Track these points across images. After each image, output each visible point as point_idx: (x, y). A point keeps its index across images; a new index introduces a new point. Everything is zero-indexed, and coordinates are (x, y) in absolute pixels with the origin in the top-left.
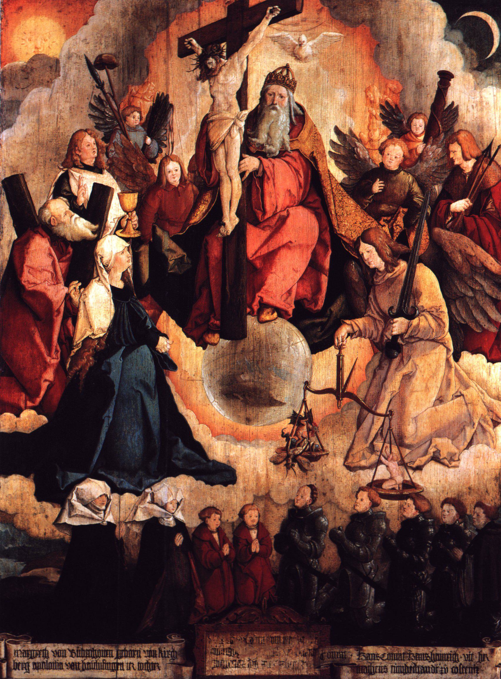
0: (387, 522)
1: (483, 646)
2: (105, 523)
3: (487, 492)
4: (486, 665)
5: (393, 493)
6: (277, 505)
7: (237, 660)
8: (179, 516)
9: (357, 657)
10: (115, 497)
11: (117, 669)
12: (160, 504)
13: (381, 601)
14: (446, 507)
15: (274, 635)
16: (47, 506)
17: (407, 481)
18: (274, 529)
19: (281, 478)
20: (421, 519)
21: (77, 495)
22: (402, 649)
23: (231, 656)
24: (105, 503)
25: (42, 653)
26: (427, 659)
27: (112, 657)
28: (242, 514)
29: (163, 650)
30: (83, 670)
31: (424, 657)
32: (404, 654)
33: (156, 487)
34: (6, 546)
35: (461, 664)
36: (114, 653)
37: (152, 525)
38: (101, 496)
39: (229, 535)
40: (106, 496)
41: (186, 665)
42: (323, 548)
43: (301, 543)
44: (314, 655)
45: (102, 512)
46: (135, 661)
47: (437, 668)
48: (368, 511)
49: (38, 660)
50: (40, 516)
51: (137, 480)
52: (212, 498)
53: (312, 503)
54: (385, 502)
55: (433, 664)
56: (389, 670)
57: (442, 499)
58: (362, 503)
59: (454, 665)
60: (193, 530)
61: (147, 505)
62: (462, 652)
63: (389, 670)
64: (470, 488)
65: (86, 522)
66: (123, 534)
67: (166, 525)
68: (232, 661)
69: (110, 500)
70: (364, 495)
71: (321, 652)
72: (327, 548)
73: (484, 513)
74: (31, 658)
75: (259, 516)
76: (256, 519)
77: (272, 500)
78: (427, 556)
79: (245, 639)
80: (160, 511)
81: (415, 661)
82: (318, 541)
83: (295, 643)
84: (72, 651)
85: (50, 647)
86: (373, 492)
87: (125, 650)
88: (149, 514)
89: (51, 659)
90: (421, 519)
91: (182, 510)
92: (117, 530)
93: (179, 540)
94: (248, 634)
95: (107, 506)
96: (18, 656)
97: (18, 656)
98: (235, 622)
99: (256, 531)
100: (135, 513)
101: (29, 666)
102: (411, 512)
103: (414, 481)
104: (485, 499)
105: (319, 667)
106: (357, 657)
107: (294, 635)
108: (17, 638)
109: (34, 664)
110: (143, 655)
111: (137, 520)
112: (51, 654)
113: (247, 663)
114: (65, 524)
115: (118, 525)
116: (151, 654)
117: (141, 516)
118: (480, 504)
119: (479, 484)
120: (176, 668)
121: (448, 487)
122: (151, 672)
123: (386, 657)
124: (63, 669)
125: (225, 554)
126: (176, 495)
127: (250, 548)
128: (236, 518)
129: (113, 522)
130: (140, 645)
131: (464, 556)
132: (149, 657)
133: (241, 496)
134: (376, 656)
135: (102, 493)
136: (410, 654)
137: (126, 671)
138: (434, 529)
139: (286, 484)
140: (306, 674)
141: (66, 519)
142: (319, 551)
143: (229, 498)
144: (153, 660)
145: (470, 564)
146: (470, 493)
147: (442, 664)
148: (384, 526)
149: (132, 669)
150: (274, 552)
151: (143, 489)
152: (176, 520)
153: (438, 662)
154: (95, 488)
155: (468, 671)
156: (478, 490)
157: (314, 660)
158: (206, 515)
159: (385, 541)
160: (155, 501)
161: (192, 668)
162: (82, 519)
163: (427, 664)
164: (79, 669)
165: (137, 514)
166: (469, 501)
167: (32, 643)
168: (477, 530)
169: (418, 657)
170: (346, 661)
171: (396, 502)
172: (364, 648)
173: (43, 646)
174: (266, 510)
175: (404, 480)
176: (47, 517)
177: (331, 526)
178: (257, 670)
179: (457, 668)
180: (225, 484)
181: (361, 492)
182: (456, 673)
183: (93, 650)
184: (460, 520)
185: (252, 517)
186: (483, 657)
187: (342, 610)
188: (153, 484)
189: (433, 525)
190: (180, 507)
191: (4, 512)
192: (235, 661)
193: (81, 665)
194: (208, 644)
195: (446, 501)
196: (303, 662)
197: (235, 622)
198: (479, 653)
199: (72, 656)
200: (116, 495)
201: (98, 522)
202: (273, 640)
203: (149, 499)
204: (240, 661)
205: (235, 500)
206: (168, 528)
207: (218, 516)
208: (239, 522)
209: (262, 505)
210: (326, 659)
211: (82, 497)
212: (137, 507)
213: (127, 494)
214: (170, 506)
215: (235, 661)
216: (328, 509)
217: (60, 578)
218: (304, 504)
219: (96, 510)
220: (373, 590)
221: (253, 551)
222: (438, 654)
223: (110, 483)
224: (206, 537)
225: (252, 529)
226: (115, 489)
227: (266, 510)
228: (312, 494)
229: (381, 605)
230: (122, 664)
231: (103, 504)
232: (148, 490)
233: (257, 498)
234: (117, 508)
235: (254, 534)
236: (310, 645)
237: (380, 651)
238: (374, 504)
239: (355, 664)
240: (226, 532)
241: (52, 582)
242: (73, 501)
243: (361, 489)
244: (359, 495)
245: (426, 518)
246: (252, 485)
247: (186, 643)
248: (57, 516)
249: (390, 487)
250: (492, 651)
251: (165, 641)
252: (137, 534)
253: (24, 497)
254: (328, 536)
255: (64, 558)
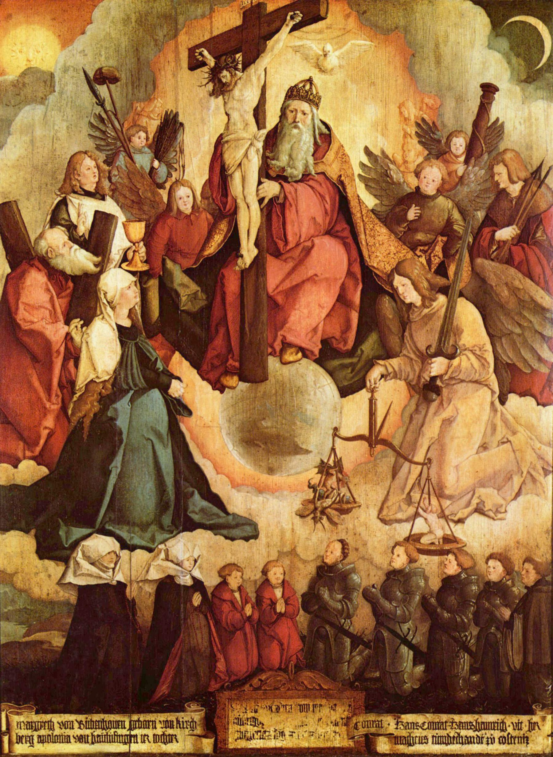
0: (426, 579)
1: (531, 712)
2: (114, 583)
3: (537, 546)
4: (537, 734)
5: (433, 548)
6: (305, 562)
7: (262, 730)
8: (197, 573)
9: (395, 726)
10: (125, 554)
11: (131, 742)
12: (175, 561)
13: (421, 663)
14: (491, 563)
15: (303, 703)
16: (50, 564)
17: (447, 535)
18: (301, 585)
19: (308, 532)
20: (463, 576)
21: (83, 553)
22: (444, 717)
23: (255, 726)
24: (114, 561)
25: (47, 724)
26: (471, 728)
27: (125, 728)
28: (265, 572)
29: (181, 720)
30: (93, 743)
31: (468, 726)
32: (446, 722)
33: (169, 543)
34: (6, 608)
35: (509, 734)
36: (127, 725)
37: (167, 585)
38: (109, 553)
39: (253, 596)
40: (115, 553)
41: (205, 736)
42: (356, 609)
43: (331, 603)
44: (346, 724)
45: (111, 570)
46: (150, 732)
47: (482, 738)
48: (406, 568)
49: (43, 732)
50: (42, 575)
51: (148, 535)
52: (233, 554)
53: (343, 559)
54: (423, 559)
55: (479, 734)
56: (430, 740)
57: (487, 555)
58: (398, 559)
59: (502, 734)
60: (212, 589)
61: (160, 562)
62: (510, 720)
63: (430, 740)
64: (518, 542)
65: (93, 582)
66: (134, 594)
67: (182, 583)
68: (257, 732)
69: (120, 557)
70: (400, 550)
71: (355, 722)
72: (360, 606)
73: (534, 569)
74: (36, 730)
75: (285, 573)
76: (282, 577)
77: (298, 555)
78: (471, 616)
79: (270, 708)
80: (175, 569)
81: (458, 731)
82: (350, 600)
83: (326, 711)
84: (80, 723)
85: (56, 718)
86: (411, 548)
87: (139, 720)
88: (164, 572)
89: (57, 731)
90: (463, 576)
91: (200, 567)
92: (128, 590)
93: (197, 600)
94: (274, 702)
95: (116, 564)
96: (21, 728)
97: (21, 728)
98: (259, 688)
99: (281, 590)
100: (147, 572)
101: (33, 739)
102: (452, 569)
103: (456, 535)
104: (535, 554)
105: (353, 738)
106: (395, 726)
107: (324, 702)
108: (20, 709)
109: (39, 737)
110: (158, 726)
111: (150, 579)
112: (56, 726)
113: (272, 734)
114: (70, 583)
115: (129, 584)
116: (168, 724)
117: (155, 575)
118: (528, 560)
119: (528, 537)
120: (196, 740)
121: (493, 541)
122: (168, 745)
123: (426, 726)
124: (70, 742)
125: (248, 615)
126: (193, 551)
127: (275, 609)
128: (259, 575)
129: (123, 580)
130: (155, 714)
131: (512, 616)
132: (166, 728)
133: (264, 551)
134: (415, 725)
135: (110, 551)
136: (452, 723)
137: (140, 744)
138: (478, 586)
139: (314, 538)
140: (338, 745)
141: (70, 578)
142: (351, 611)
143: (250, 555)
144: (170, 731)
145: (518, 625)
146: (518, 547)
147: (488, 733)
148: (422, 583)
149: (147, 741)
150: (301, 612)
151: (156, 544)
152: (194, 578)
153: (483, 732)
154: (101, 545)
155: (516, 741)
156: (527, 544)
157: (348, 731)
158: (227, 572)
159: (424, 601)
160: (170, 558)
161: (213, 740)
162: (89, 578)
163: (471, 733)
164: (88, 742)
165: (150, 572)
166: (517, 557)
167: (36, 714)
168: (526, 587)
169: (461, 725)
170: (382, 731)
171: (436, 559)
172: (403, 716)
173: (48, 717)
174: (292, 567)
175: (444, 534)
176: (49, 576)
177: (364, 584)
178: (284, 742)
179: (504, 737)
180: (246, 539)
181: (397, 547)
182: (504, 744)
183: (103, 721)
184: (508, 577)
185: (276, 575)
186: (533, 726)
187: (377, 674)
188: (167, 540)
189: (477, 583)
190: (197, 564)
191: (3, 572)
192: (260, 731)
193: (90, 738)
194: (230, 713)
195: (491, 556)
196: (335, 732)
197: (259, 688)
198: (529, 721)
199: (80, 728)
200: (126, 552)
201: (106, 582)
202: (303, 708)
203: (163, 555)
204: (265, 732)
205: (257, 557)
206: (185, 587)
207: (240, 574)
208: (262, 580)
209: (287, 562)
210: (361, 729)
211: (88, 554)
212: (150, 565)
213: (138, 551)
214: (187, 564)
215: (260, 731)
216: (362, 566)
217: (66, 643)
218: (334, 560)
219: (104, 569)
220: (411, 653)
221: (278, 610)
222: (483, 723)
223: (119, 539)
224: (226, 596)
225: (277, 587)
226: (124, 545)
227: (292, 567)
228: (343, 549)
229: (420, 668)
230: (136, 736)
231: (111, 562)
232: (162, 546)
233: (281, 554)
234: (127, 566)
235: (278, 593)
236: (341, 712)
237: (419, 718)
238: (412, 560)
239: (393, 734)
240: (248, 590)
241: (57, 647)
242: (78, 559)
243: (397, 544)
244: (395, 551)
245: (469, 576)
246: (276, 539)
247: (206, 713)
248: (60, 575)
249: (430, 542)
250: (544, 719)
251: (183, 710)
252: (150, 594)
253: (24, 555)
254: (361, 595)
255: (70, 621)
